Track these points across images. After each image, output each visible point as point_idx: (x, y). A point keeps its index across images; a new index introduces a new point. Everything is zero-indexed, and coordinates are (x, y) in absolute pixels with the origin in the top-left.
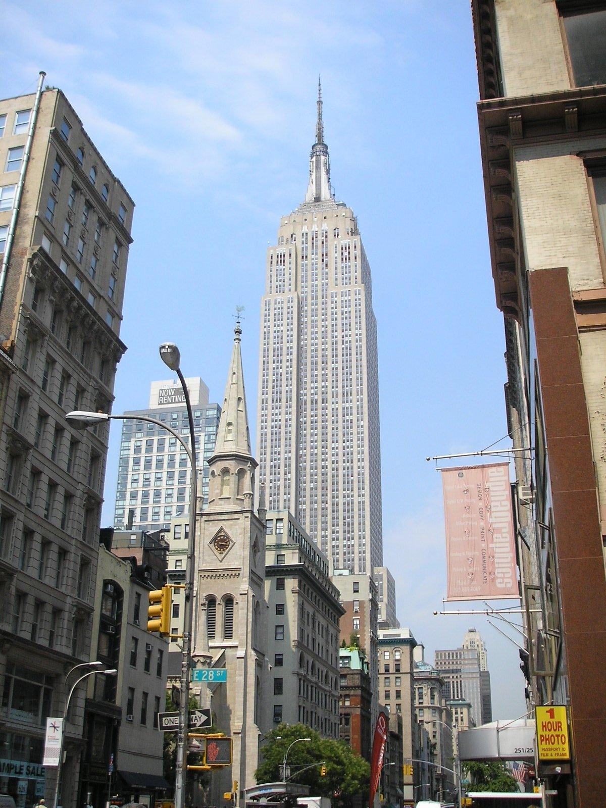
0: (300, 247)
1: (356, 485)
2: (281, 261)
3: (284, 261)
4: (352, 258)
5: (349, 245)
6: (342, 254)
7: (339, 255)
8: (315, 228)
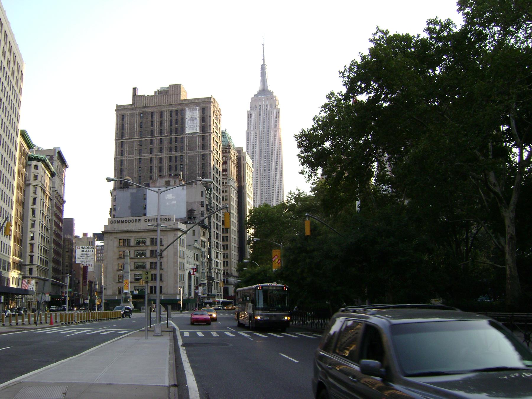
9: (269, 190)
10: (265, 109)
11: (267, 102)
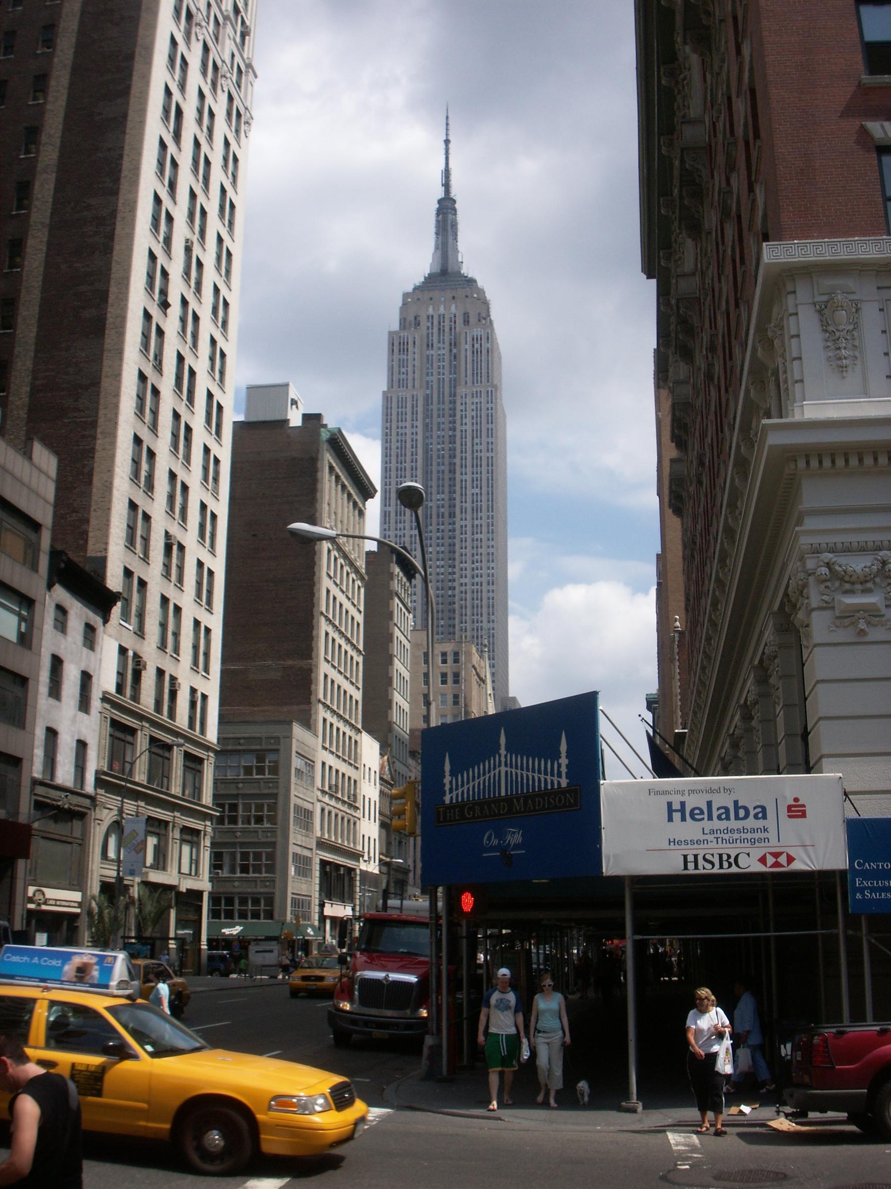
0: (425, 332)
1: (485, 610)
2: (404, 349)
3: (407, 351)
5: (481, 335)
6: (473, 346)
7: (468, 346)
8: (442, 310)
9: (450, 577)
10: (447, 329)
11: (453, 307)
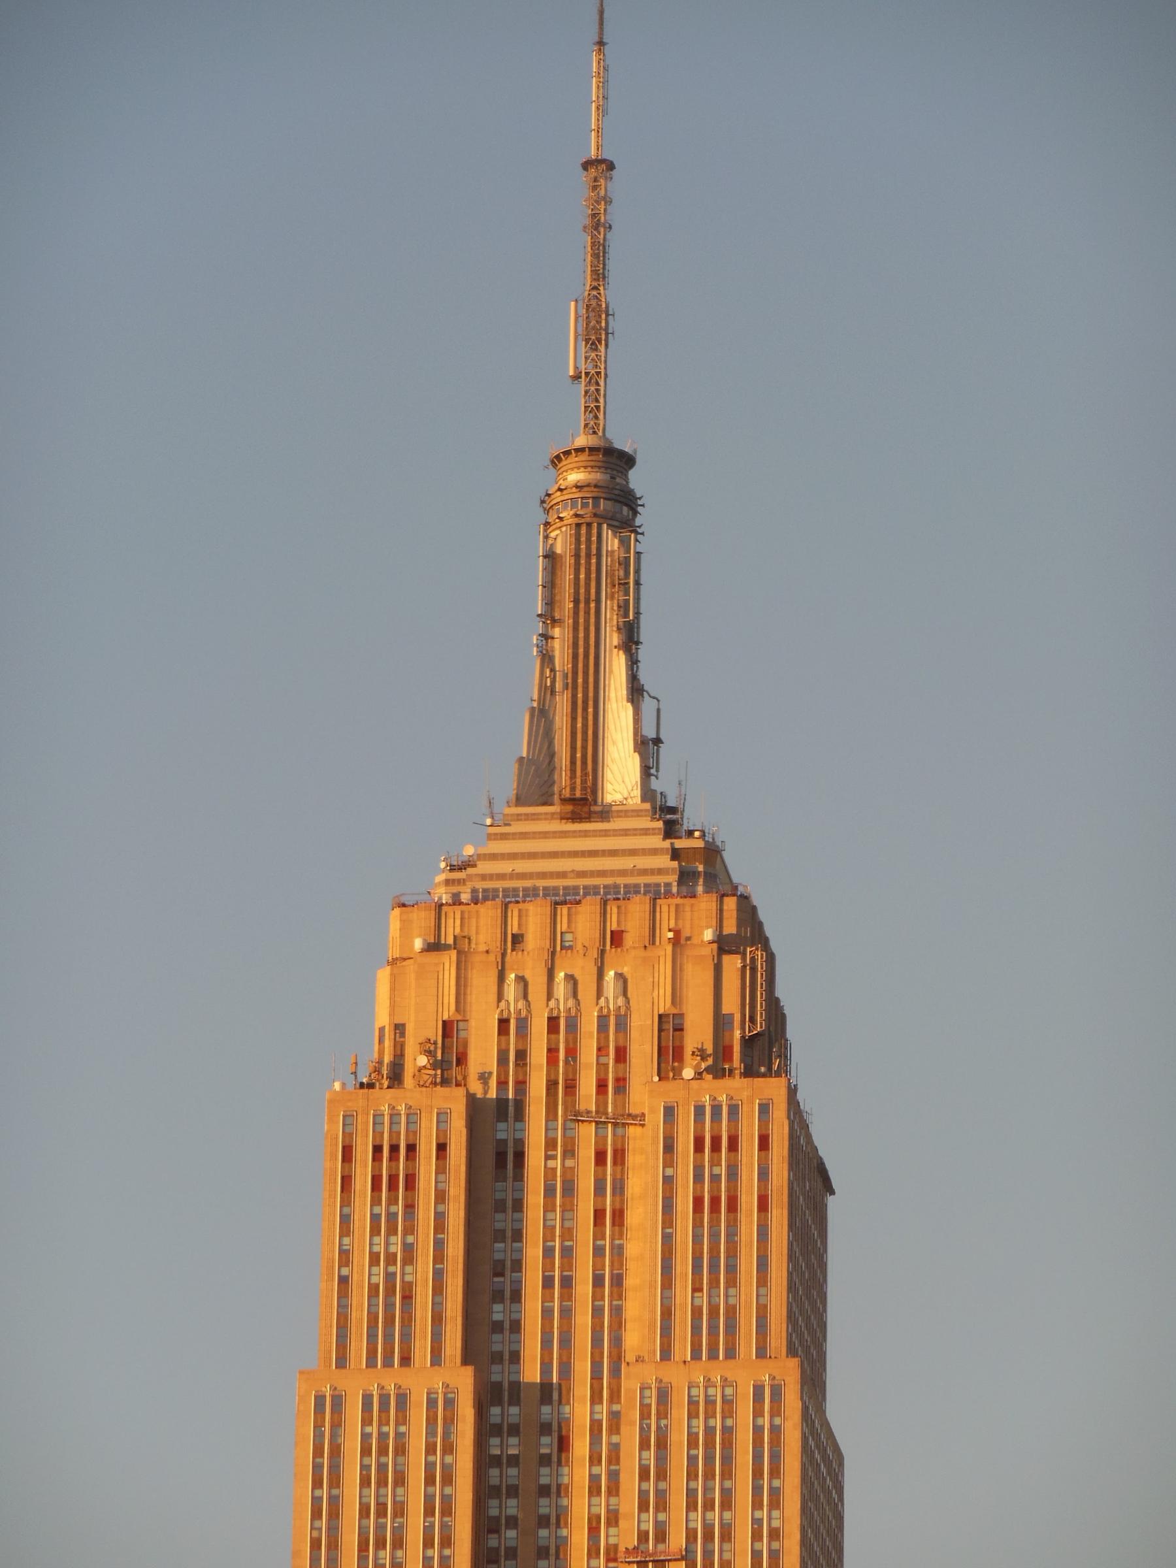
2: (393, 1180)
4: (749, 1200)
